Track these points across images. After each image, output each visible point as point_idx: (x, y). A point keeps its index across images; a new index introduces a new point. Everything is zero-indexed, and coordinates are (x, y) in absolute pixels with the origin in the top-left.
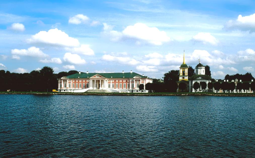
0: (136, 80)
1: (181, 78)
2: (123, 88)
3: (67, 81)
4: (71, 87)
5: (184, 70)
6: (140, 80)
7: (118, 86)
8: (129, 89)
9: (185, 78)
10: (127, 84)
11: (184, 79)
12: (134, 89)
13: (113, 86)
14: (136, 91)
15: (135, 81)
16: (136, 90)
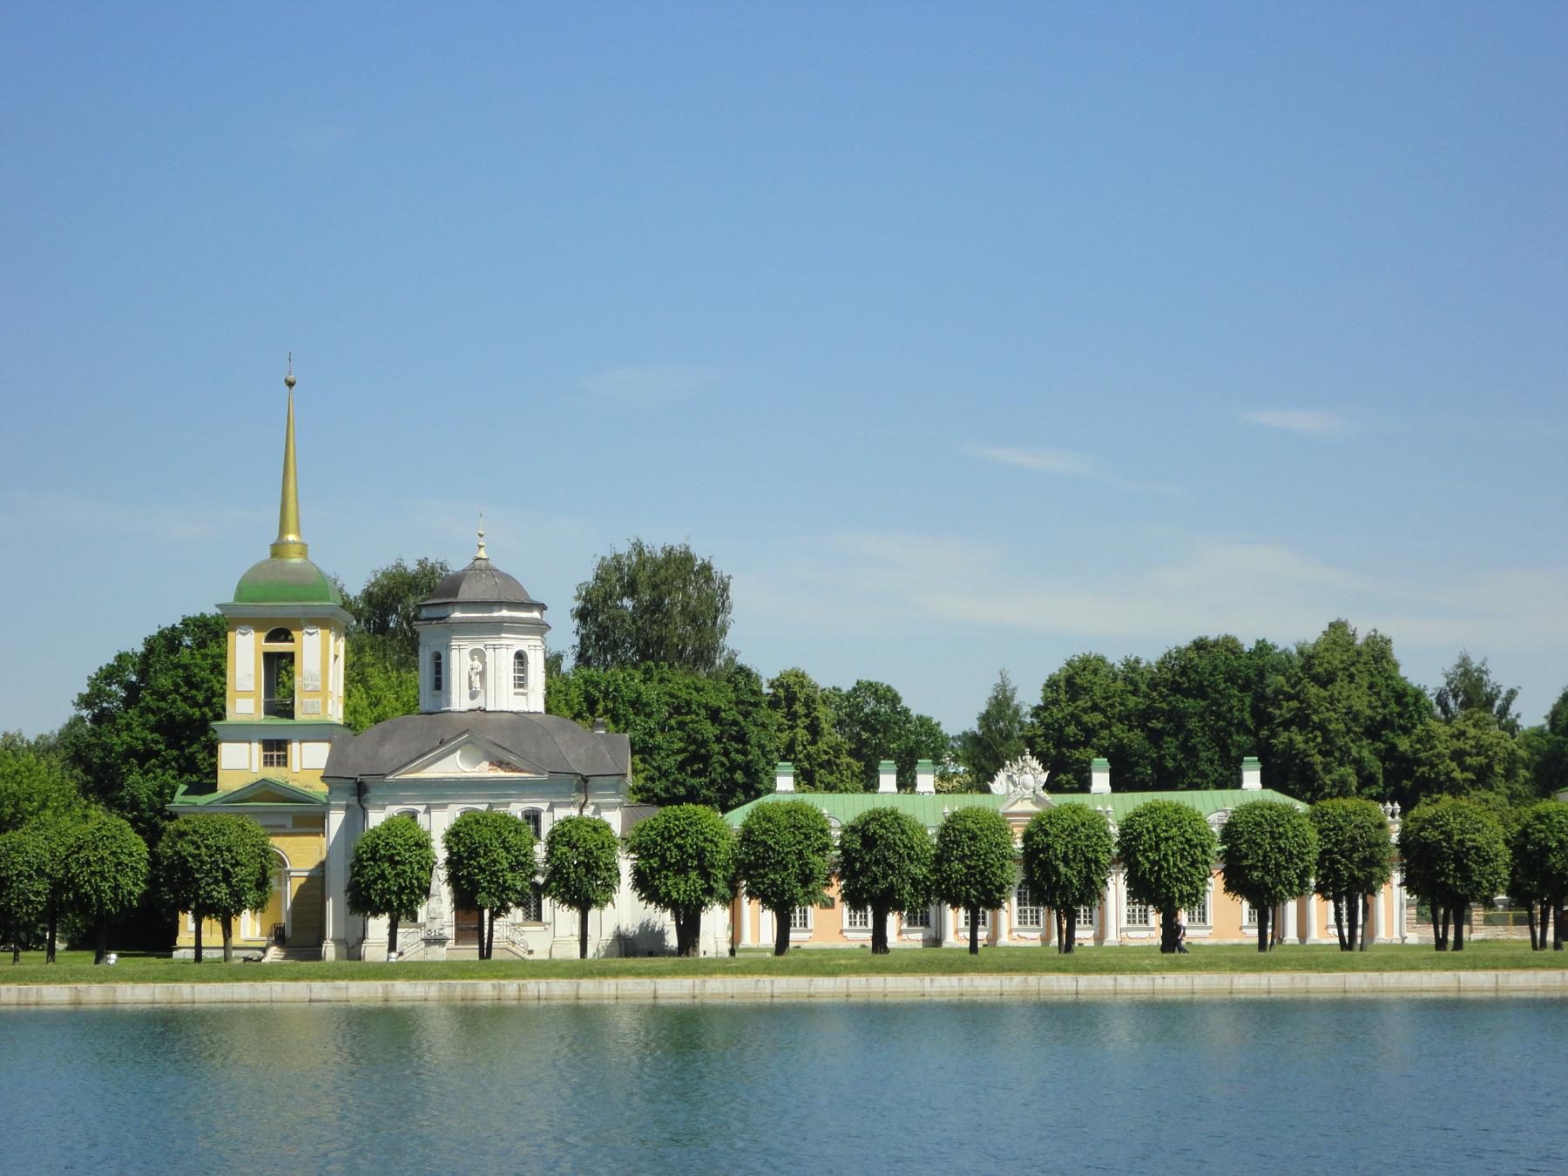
1: (238, 762)
9: (294, 749)
11: (274, 774)
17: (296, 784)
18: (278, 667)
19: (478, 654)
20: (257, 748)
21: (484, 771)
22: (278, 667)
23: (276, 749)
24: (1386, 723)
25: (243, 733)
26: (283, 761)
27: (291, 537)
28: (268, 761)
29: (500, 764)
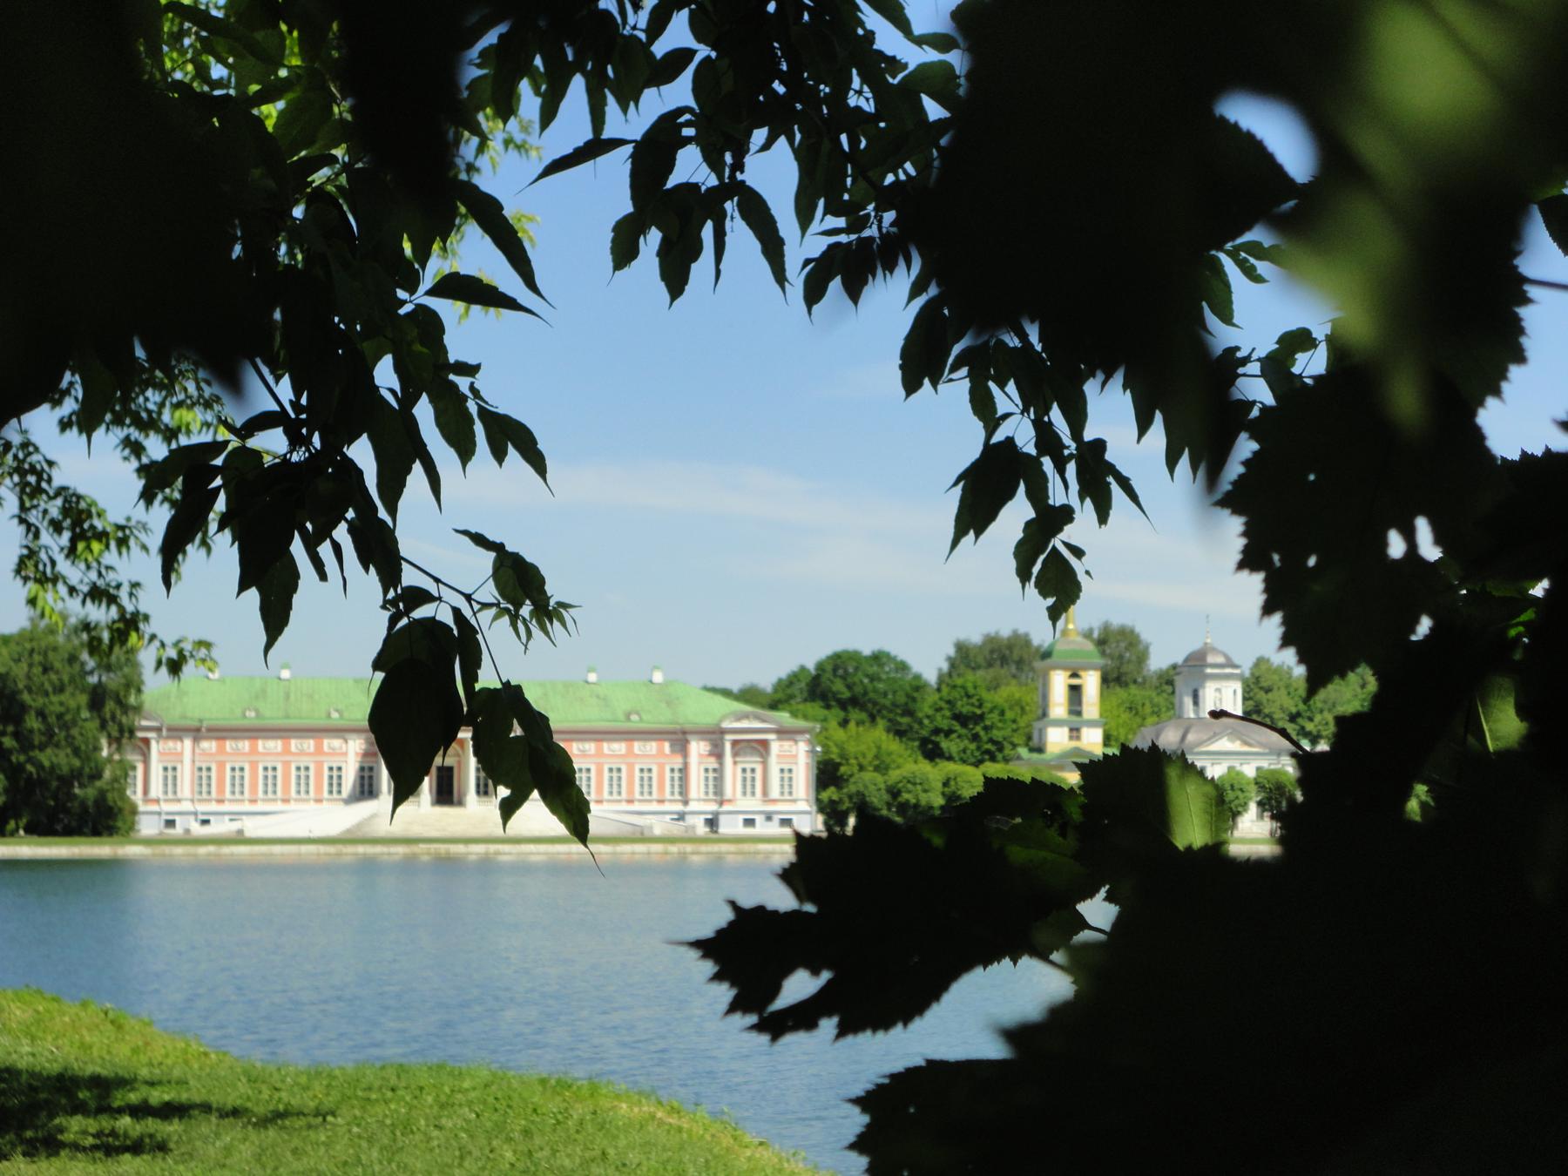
0: (735, 743)
1: (1057, 739)
2: (228, 795)
3: (153, 744)
4: (185, 788)
5: (1075, 681)
6: (765, 744)
7: (624, 783)
8: (686, 803)
9: (1085, 731)
10: (606, 768)
11: (1074, 744)
12: (726, 808)
13: (166, 785)
14: (741, 823)
15: (728, 746)
16: (741, 817)
17: (1088, 749)
18: (1075, 691)
19: (1218, 690)
20: (1066, 730)
21: (1237, 746)
22: (1075, 691)
23: (1075, 732)
24: (1298, 714)
25: (1058, 723)
26: (1078, 738)
27: (1071, 626)
28: (1071, 738)
29: (1246, 743)
